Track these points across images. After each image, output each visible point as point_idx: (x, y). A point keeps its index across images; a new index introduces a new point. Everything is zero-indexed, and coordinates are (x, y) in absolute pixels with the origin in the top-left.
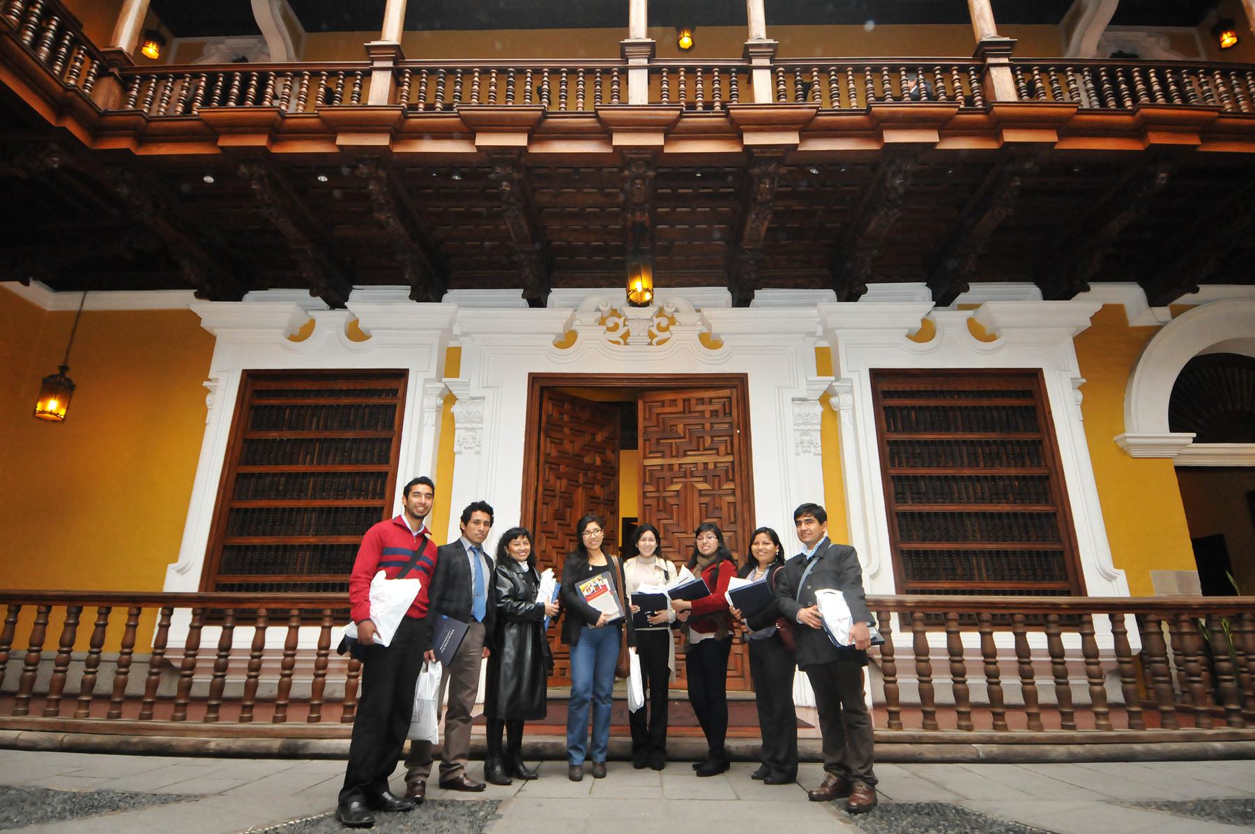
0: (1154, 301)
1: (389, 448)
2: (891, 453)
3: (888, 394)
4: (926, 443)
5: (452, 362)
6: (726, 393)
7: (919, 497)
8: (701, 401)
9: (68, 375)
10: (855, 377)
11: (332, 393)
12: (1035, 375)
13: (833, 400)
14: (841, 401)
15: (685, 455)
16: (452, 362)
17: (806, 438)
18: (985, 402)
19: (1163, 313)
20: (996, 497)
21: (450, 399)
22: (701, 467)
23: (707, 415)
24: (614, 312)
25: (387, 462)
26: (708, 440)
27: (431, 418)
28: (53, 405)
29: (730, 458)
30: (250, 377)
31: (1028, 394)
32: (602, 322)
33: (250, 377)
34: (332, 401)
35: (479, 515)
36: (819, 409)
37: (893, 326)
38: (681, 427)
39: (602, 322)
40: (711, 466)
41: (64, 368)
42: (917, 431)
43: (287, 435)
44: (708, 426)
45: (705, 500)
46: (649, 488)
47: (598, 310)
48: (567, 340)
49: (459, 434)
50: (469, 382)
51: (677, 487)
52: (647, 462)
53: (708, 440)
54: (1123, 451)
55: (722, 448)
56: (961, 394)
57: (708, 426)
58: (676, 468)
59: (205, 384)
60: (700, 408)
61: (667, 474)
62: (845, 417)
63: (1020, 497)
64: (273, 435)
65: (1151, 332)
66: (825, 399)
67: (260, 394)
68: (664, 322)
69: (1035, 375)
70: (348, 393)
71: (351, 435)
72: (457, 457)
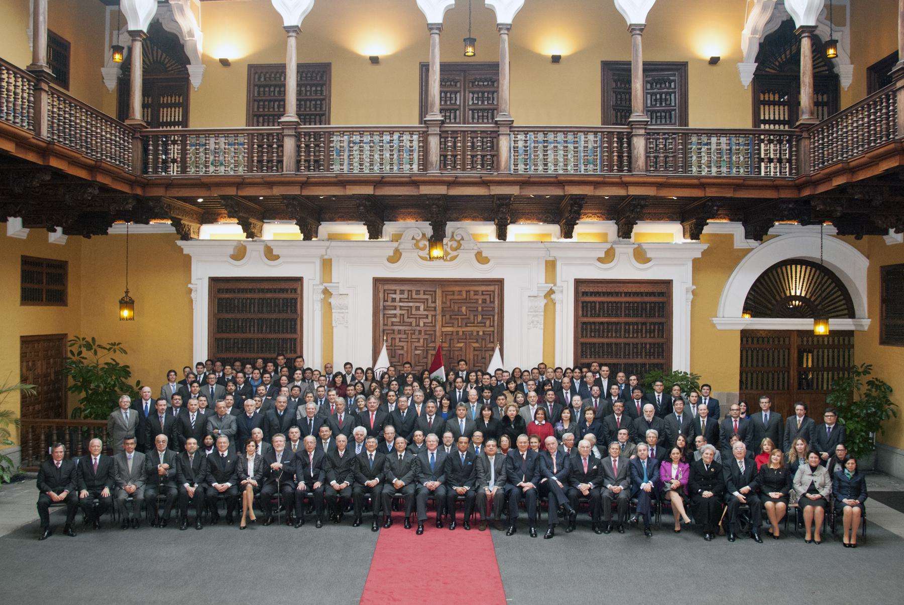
0: (747, 236)
1: (296, 324)
3: (585, 294)
4: (602, 323)
5: (327, 264)
6: (491, 288)
9: (129, 295)
10: (565, 285)
12: (668, 283)
15: (466, 326)
16: (327, 264)
17: (536, 319)
18: (638, 299)
19: (752, 243)
21: (327, 292)
22: (475, 333)
23: (480, 302)
25: (295, 332)
27: (318, 307)
28: (126, 313)
29: (492, 329)
30: (213, 281)
31: (661, 294)
33: (213, 281)
34: (261, 296)
35: (348, 366)
37: (590, 249)
38: (464, 309)
40: (481, 333)
41: (127, 292)
42: (599, 316)
43: (239, 316)
44: (480, 309)
45: (476, 353)
48: (395, 258)
49: (335, 316)
50: (338, 273)
51: (462, 345)
53: (480, 318)
55: (488, 323)
56: (627, 294)
57: (480, 309)
58: (461, 333)
59: (190, 286)
60: (476, 297)
62: (557, 305)
63: (650, 354)
64: (230, 316)
65: (746, 252)
67: (219, 291)
68: (455, 244)
69: (668, 283)
70: (269, 291)
71: (274, 316)
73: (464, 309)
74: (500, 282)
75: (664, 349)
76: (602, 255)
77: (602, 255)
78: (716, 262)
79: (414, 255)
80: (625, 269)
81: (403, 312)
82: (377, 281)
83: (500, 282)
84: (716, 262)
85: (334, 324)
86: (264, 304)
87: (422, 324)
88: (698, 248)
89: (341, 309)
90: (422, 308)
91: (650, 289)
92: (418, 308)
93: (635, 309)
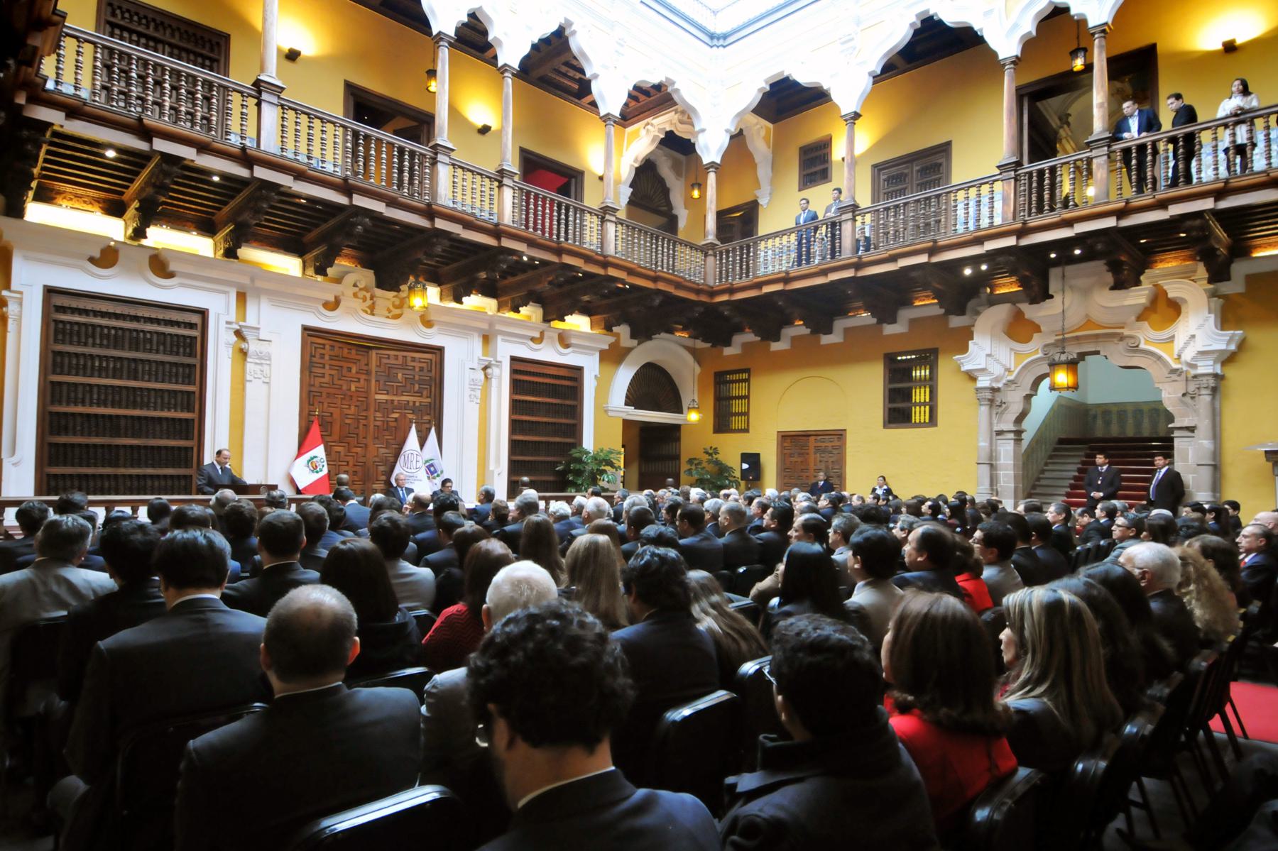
0: (633, 336)
2: (515, 406)
7: (523, 432)
8: (413, 359)
11: (136, 318)
13: (489, 371)
14: (494, 371)
19: (635, 342)
20: (555, 434)
21: (238, 333)
24: (366, 289)
26: (417, 387)
30: (50, 292)
31: (575, 379)
32: (355, 295)
33: (50, 292)
36: (481, 375)
39: (355, 295)
46: (378, 414)
47: (355, 285)
51: (396, 415)
52: (378, 397)
53: (417, 387)
54: (606, 411)
55: (425, 393)
59: (5, 293)
61: (389, 406)
62: (494, 382)
65: (629, 350)
66: (485, 369)
69: (580, 370)
72: (248, 384)
73: (400, 375)
74: (440, 350)
75: (575, 430)
76: (537, 335)
77: (537, 335)
78: (613, 357)
79: (358, 304)
80: (549, 353)
81: (333, 372)
82: (306, 329)
83: (440, 350)
84: (613, 357)
85: (248, 378)
86: (117, 338)
87: (353, 388)
88: (605, 342)
89: (261, 358)
90: (354, 371)
91: (562, 372)
92: (349, 369)
93: (553, 391)
